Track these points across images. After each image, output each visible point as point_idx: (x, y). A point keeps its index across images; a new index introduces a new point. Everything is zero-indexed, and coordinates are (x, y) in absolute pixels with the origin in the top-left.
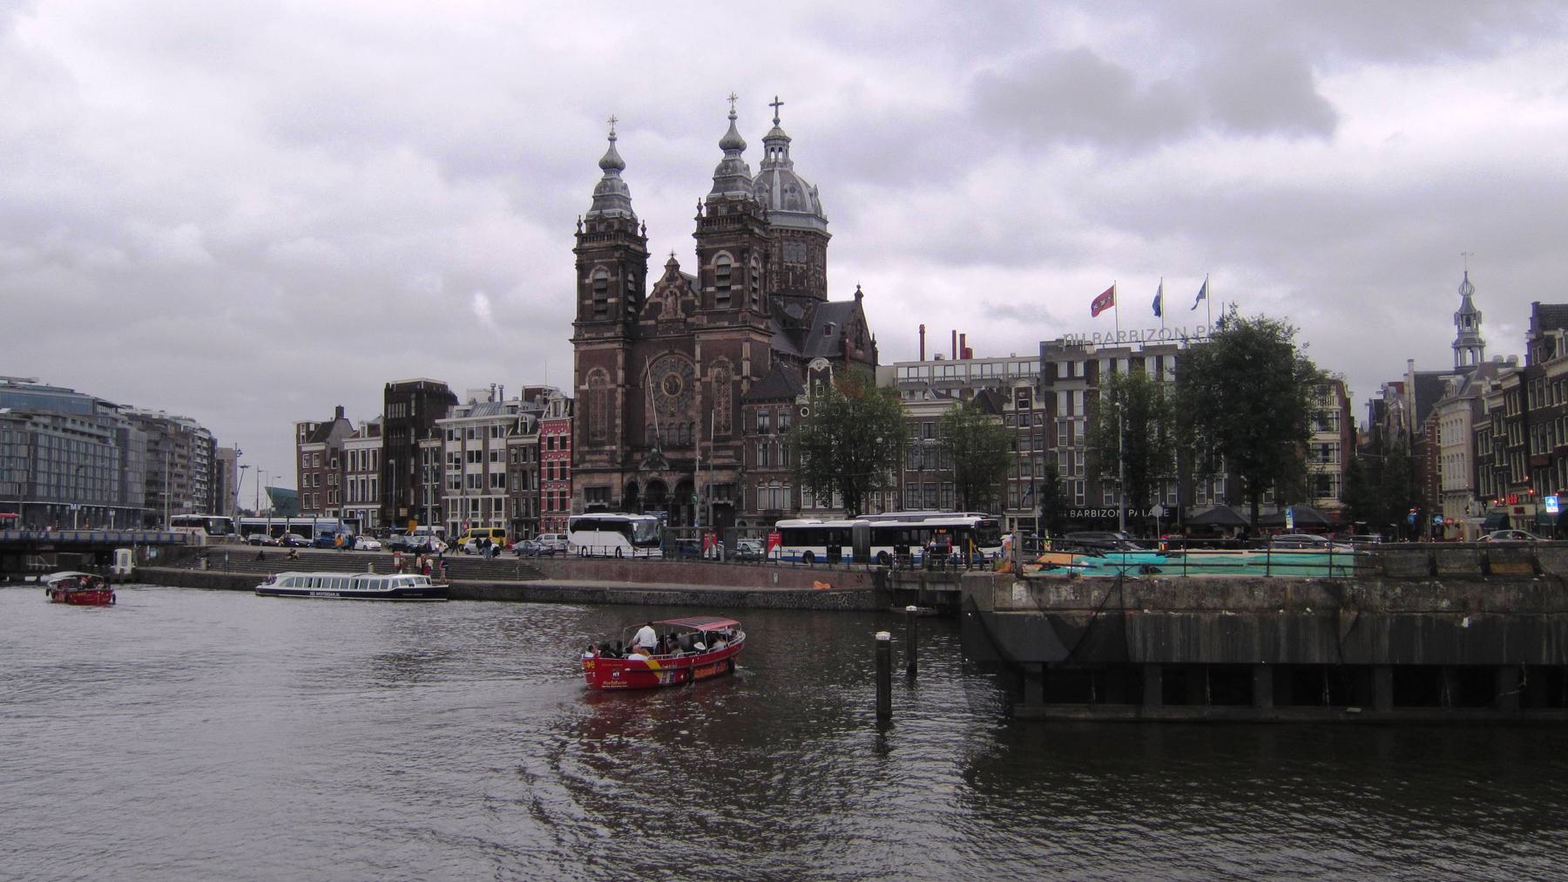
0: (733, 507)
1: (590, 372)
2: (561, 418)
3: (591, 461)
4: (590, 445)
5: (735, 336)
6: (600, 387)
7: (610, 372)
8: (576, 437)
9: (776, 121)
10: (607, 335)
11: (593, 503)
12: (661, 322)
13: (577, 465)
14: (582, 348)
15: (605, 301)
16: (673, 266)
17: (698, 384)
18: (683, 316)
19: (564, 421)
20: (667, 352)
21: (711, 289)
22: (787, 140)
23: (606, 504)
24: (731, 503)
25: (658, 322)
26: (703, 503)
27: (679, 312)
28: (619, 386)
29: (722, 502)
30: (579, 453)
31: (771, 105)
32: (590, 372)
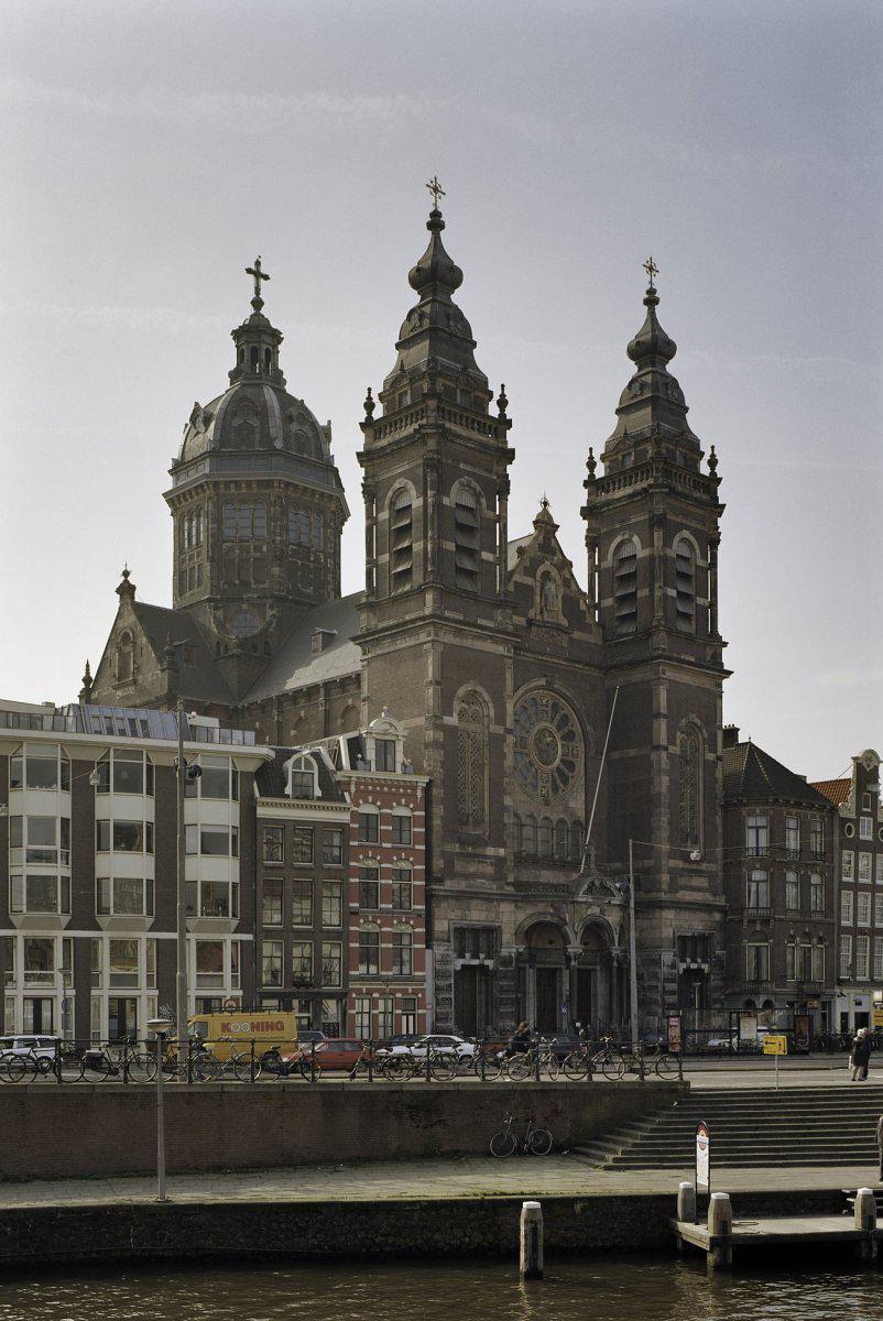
0: (708, 974)
1: (461, 692)
2: (398, 774)
3: (467, 876)
4: (463, 843)
5: (707, 683)
6: (472, 727)
7: (492, 694)
8: (437, 822)
9: (257, 303)
10: (481, 622)
11: (469, 960)
12: (543, 625)
13: (440, 881)
14: (448, 638)
15: (479, 552)
16: (546, 525)
17: (664, 755)
18: (565, 622)
19: (414, 787)
20: (542, 682)
21: (672, 593)
22: (276, 337)
23: (489, 963)
24: (705, 967)
25: (530, 623)
26: (673, 966)
27: (560, 613)
28: (509, 731)
29: (694, 966)
30: (443, 854)
31: (249, 271)
32: (461, 692)
